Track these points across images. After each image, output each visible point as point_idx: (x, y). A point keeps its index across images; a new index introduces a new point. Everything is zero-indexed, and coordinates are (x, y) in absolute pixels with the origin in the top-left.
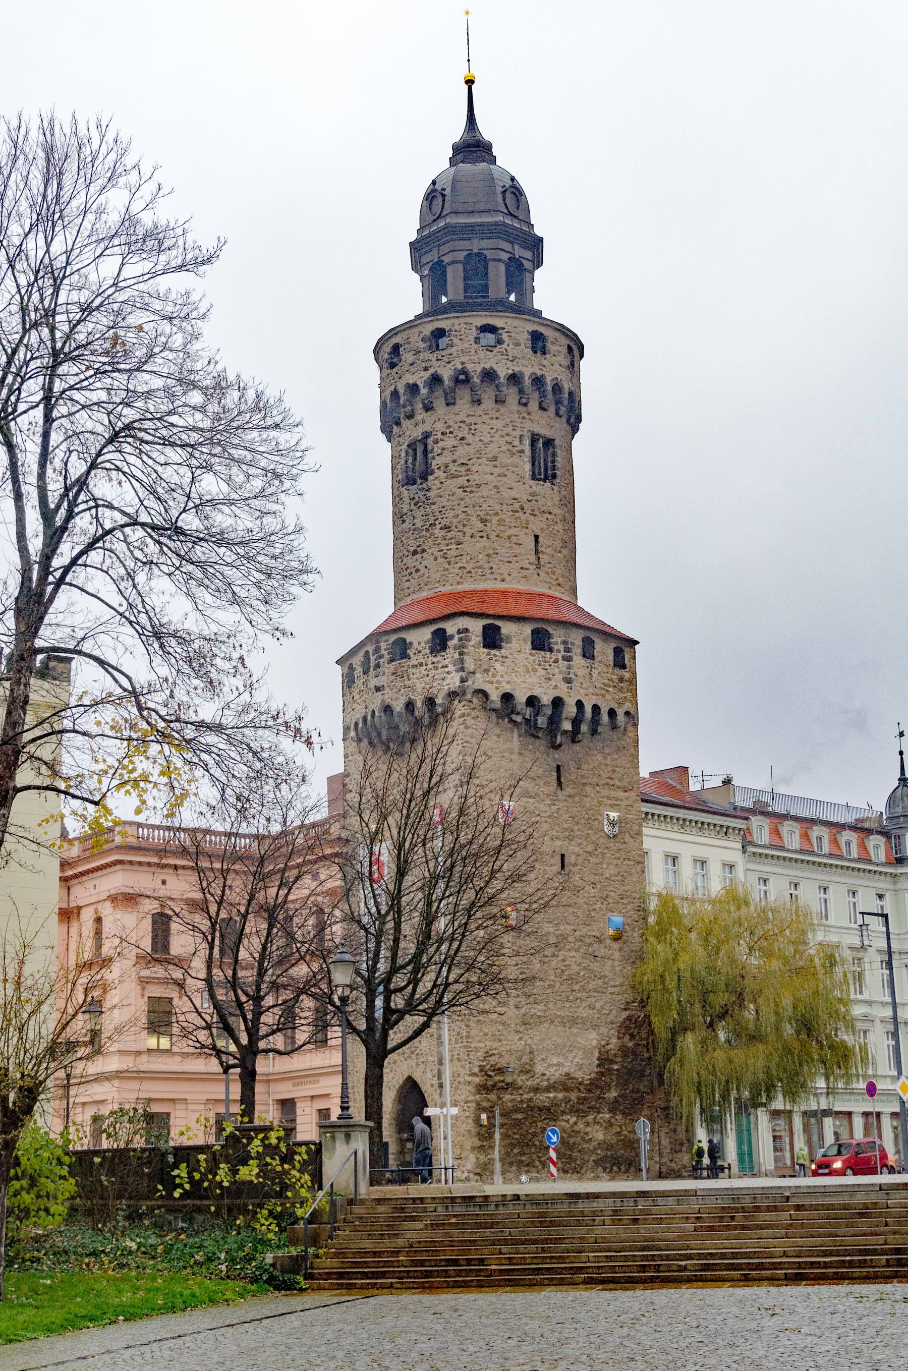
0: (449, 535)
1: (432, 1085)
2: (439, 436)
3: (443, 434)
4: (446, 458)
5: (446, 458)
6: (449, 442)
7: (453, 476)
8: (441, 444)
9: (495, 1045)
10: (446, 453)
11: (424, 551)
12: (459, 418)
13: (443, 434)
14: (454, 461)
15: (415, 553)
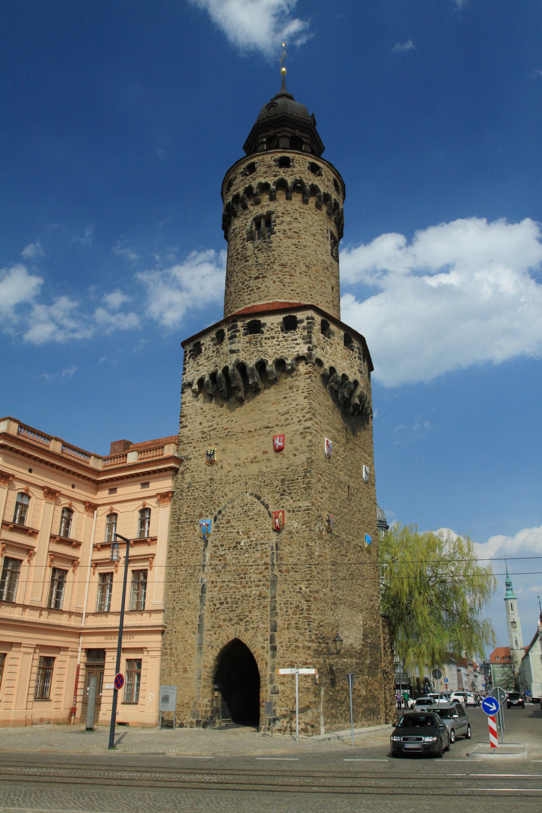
0: (285, 270)
1: (263, 648)
2: (280, 214)
3: (283, 213)
4: (285, 227)
5: (285, 227)
6: (287, 219)
7: (289, 237)
8: (281, 219)
9: (323, 618)
10: (284, 224)
11: (264, 277)
12: (294, 207)
13: (283, 213)
14: (290, 229)
15: (257, 278)
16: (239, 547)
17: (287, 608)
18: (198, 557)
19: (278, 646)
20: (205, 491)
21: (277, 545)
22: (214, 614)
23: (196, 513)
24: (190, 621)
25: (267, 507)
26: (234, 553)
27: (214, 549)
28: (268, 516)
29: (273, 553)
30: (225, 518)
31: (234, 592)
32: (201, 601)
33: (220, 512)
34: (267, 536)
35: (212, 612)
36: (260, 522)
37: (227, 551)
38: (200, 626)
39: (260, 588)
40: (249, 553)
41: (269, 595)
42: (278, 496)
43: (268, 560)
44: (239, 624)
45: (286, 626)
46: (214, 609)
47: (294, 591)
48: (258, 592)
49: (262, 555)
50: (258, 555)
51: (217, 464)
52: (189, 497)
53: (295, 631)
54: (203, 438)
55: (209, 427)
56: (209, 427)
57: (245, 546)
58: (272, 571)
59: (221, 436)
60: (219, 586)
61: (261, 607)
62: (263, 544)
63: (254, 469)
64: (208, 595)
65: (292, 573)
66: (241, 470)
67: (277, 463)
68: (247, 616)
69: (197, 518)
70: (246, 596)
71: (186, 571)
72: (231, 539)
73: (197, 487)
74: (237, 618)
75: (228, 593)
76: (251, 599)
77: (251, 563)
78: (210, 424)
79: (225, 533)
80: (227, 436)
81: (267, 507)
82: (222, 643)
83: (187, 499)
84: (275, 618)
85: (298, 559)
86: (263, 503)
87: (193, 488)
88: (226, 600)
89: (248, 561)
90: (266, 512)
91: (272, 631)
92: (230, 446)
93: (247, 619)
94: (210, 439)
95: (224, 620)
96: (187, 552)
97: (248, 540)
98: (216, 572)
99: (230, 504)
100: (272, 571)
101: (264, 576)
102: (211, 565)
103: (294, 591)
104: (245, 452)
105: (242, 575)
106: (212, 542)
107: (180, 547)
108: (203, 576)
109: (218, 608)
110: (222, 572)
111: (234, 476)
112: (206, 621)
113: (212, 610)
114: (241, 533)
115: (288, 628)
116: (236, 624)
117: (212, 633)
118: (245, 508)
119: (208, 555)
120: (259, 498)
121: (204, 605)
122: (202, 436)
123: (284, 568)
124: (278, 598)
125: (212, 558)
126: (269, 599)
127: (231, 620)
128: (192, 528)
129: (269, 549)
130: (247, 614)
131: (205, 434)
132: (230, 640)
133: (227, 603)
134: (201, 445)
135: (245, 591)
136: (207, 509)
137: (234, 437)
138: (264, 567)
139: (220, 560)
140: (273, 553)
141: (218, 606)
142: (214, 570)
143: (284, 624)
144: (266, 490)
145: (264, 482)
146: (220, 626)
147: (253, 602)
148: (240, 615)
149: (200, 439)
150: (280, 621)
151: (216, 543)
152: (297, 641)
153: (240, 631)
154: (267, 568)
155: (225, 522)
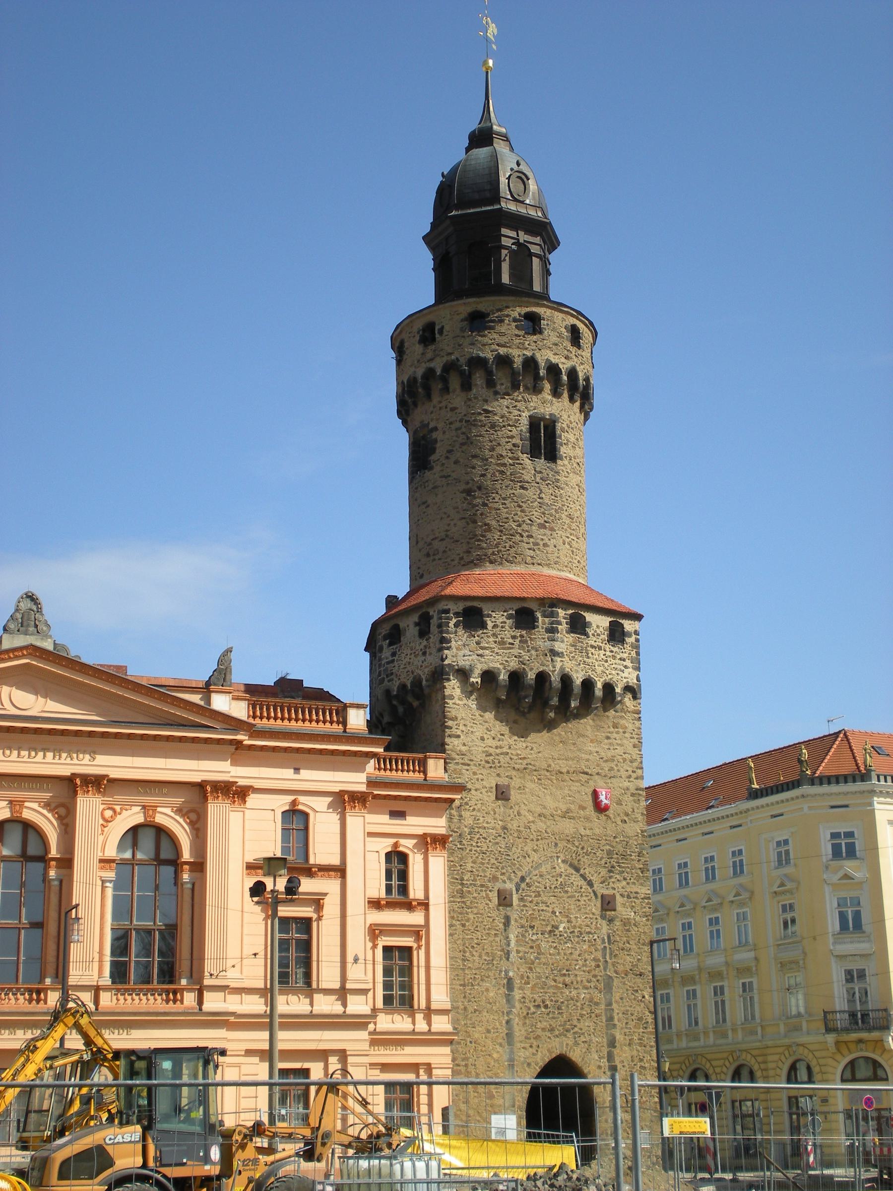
1: (600, 1067)
16: (557, 932)
17: (627, 1019)
18: (498, 939)
19: (619, 1066)
20: (497, 843)
21: (609, 937)
22: (527, 1021)
23: (488, 874)
24: (493, 1028)
25: (590, 884)
26: (550, 939)
27: (520, 930)
28: (594, 898)
29: (605, 947)
30: (533, 888)
31: (554, 993)
32: (508, 1001)
33: (523, 879)
35: (525, 1017)
36: (583, 902)
37: (540, 935)
38: (509, 1036)
39: (591, 991)
40: (572, 943)
41: (603, 1001)
43: (599, 955)
44: (565, 1036)
45: (628, 1042)
46: (528, 1014)
47: (635, 999)
48: (588, 996)
51: (511, 807)
52: (474, 849)
53: (639, 1048)
54: (488, 762)
55: (497, 748)
56: (497, 748)
57: (566, 932)
58: (605, 969)
59: (517, 766)
60: (532, 983)
61: (593, 1015)
62: (589, 933)
63: (568, 827)
64: (517, 994)
65: (630, 976)
66: (548, 824)
67: (598, 824)
68: (575, 1026)
69: (489, 881)
70: (572, 999)
72: (544, 920)
73: (484, 835)
74: (561, 1028)
75: (546, 993)
76: (579, 1004)
77: (575, 956)
78: (499, 744)
79: (534, 910)
80: (525, 769)
81: (590, 884)
82: (542, 1059)
83: (471, 850)
84: (613, 1031)
85: (639, 960)
86: (583, 877)
87: (478, 836)
88: (543, 1002)
89: (571, 953)
90: (590, 890)
91: (609, 1046)
92: (530, 785)
93: (576, 1029)
94: (500, 767)
95: (543, 1029)
96: (478, 929)
98: (526, 963)
99: (535, 869)
100: (605, 969)
101: (595, 976)
103: (635, 999)
104: (553, 801)
105: (564, 972)
106: (516, 921)
107: (468, 920)
109: (534, 1013)
111: (539, 831)
112: (516, 1028)
113: (525, 1014)
114: (557, 914)
115: (629, 1045)
116: (560, 1035)
117: (527, 1045)
118: (560, 880)
120: (577, 870)
121: (514, 1007)
122: (487, 758)
123: (620, 968)
124: (614, 1006)
126: (603, 1007)
127: (552, 1030)
129: (599, 941)
130: (575, 1022)
131: (491, 758)
132: (554, 1056)
133: (546, 1007)
134: (485, 772)
135: (570, 992)
136: (504, 871)
137: (535, 773)
138: (593, 964)
139: (532, 947)
140: (605, 947)
141: (533, 1009)
143: (625, 1039)
144: (585, 860)
145: (583, 848)
146: (537, 1038)
147: (582, 1009)
148: (565, 1024)
149: (483, 762)
150: (619, 1037)
151: (523, 921)
152: (641, 1060)
153: (567, 1044)
154: (598, 966)
155: (533, 895)
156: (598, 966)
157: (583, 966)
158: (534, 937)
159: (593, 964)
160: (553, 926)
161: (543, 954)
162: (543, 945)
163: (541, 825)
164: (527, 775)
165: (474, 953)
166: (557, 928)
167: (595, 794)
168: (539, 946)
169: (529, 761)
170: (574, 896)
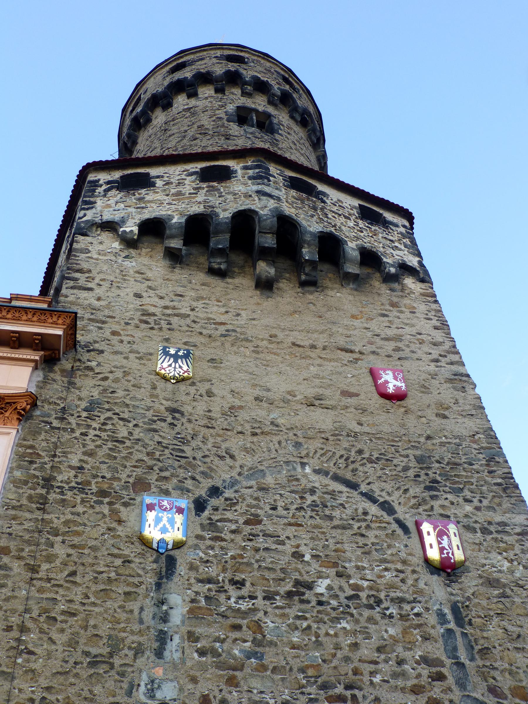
16: (308, 595)
18: (135, 606)
25: (387, 507)
29: (450, 631)
34: (410, 582)
37: (260, 602)
42: (416, 490)
43: (437, 650)
49: (405, 632)
50: (392, 631)
58: (462, 684)
63: (323, 420)
71: (73, 643)
81: (387, 507)
86: (369, 497)
89: (355, 646)
96: (78, 579)
97: (337, 582)
102: (192, 637)
106: (192, 567)
107: (50, 559)
108: (159, 672)
110: (247, 670)
114: (307, 558)
119: (178, 604)
120: (353, 486)
125: (194, 613)
128: (106, 511)
129: (432, 619)
138: (425, 671)
139: (237, 627)
142: (207, 659)
151: (213, 571)
154: (440, 677)
155: (241, 520)
156: (440, 677)
157: (395, 675)
158: (244, 606)
159: (425, 671)
160: (297, 583)
161: (272, 644)
162: (269, 624)
163: (260, 413)
164: (228, 345)
165: (55, 636)
166: (310, 586)
167: (374, 374)
168: (258, 627)
169: (230, 327)
170: (350, 527)
